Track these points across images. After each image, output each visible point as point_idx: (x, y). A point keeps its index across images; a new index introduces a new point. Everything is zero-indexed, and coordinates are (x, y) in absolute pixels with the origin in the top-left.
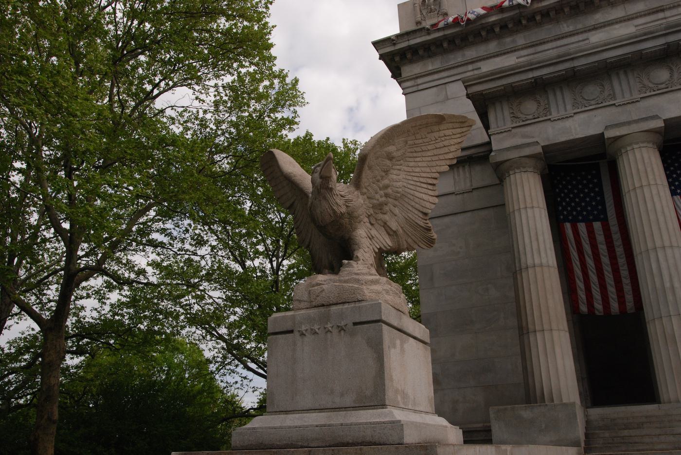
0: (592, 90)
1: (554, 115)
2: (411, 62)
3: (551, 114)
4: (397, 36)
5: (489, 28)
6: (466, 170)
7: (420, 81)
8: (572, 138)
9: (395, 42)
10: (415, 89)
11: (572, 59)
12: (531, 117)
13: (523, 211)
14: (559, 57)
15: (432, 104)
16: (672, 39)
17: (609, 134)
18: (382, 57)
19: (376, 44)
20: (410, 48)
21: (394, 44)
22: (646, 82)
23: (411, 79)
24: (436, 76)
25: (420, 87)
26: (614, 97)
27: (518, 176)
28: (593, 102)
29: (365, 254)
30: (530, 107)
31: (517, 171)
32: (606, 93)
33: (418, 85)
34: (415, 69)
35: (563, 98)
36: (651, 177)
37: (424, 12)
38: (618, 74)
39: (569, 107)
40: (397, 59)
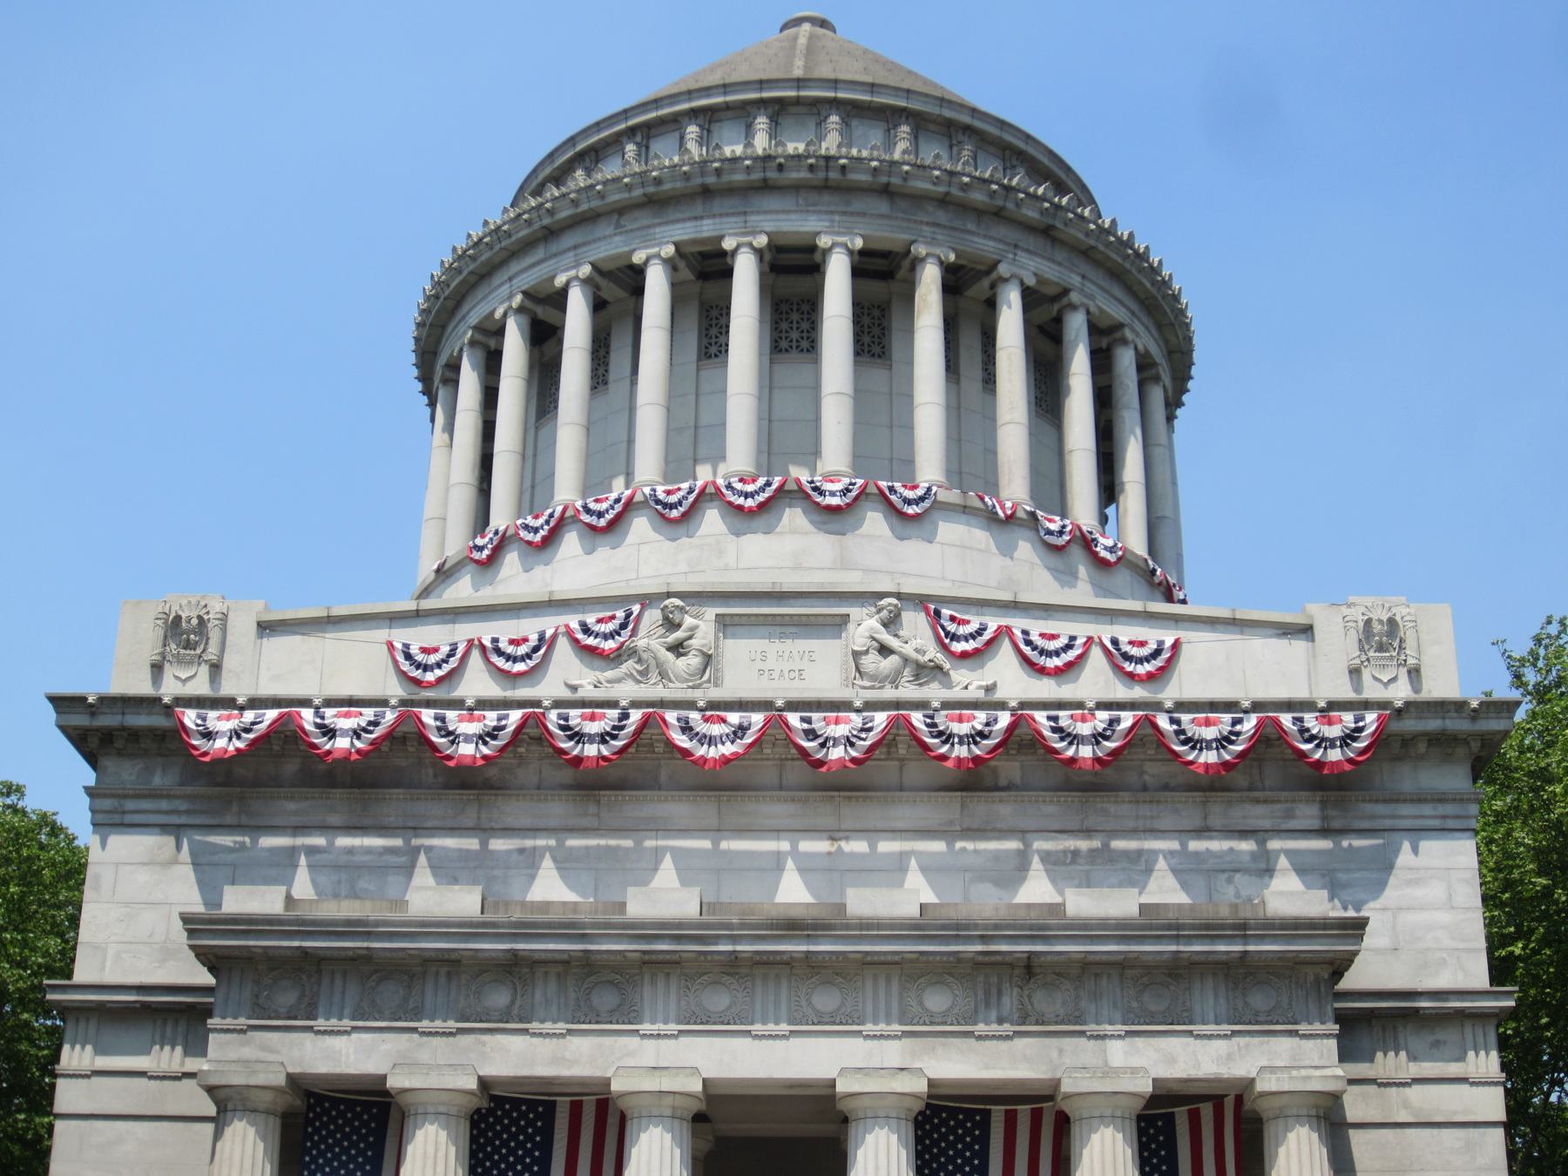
0: (391, 993)
2: (121, 754)
5: (288, 733)
6: (180, 1029)
7: (130, 805)
8: (338, 1070)
9: (94, 709)
10: (117, 818)
11: (369, 933)
14: (349, 922)
17: (393, 1083)
18: (63, 729)
19: (59, 702)
20: (123, 728)
21: (93, 714)
23: (113, 796)
24: (164, 805)
25: (128, 819)
33: (124, 812)
34: (126, 772)
35: (343, 993)
40: (94, 742)
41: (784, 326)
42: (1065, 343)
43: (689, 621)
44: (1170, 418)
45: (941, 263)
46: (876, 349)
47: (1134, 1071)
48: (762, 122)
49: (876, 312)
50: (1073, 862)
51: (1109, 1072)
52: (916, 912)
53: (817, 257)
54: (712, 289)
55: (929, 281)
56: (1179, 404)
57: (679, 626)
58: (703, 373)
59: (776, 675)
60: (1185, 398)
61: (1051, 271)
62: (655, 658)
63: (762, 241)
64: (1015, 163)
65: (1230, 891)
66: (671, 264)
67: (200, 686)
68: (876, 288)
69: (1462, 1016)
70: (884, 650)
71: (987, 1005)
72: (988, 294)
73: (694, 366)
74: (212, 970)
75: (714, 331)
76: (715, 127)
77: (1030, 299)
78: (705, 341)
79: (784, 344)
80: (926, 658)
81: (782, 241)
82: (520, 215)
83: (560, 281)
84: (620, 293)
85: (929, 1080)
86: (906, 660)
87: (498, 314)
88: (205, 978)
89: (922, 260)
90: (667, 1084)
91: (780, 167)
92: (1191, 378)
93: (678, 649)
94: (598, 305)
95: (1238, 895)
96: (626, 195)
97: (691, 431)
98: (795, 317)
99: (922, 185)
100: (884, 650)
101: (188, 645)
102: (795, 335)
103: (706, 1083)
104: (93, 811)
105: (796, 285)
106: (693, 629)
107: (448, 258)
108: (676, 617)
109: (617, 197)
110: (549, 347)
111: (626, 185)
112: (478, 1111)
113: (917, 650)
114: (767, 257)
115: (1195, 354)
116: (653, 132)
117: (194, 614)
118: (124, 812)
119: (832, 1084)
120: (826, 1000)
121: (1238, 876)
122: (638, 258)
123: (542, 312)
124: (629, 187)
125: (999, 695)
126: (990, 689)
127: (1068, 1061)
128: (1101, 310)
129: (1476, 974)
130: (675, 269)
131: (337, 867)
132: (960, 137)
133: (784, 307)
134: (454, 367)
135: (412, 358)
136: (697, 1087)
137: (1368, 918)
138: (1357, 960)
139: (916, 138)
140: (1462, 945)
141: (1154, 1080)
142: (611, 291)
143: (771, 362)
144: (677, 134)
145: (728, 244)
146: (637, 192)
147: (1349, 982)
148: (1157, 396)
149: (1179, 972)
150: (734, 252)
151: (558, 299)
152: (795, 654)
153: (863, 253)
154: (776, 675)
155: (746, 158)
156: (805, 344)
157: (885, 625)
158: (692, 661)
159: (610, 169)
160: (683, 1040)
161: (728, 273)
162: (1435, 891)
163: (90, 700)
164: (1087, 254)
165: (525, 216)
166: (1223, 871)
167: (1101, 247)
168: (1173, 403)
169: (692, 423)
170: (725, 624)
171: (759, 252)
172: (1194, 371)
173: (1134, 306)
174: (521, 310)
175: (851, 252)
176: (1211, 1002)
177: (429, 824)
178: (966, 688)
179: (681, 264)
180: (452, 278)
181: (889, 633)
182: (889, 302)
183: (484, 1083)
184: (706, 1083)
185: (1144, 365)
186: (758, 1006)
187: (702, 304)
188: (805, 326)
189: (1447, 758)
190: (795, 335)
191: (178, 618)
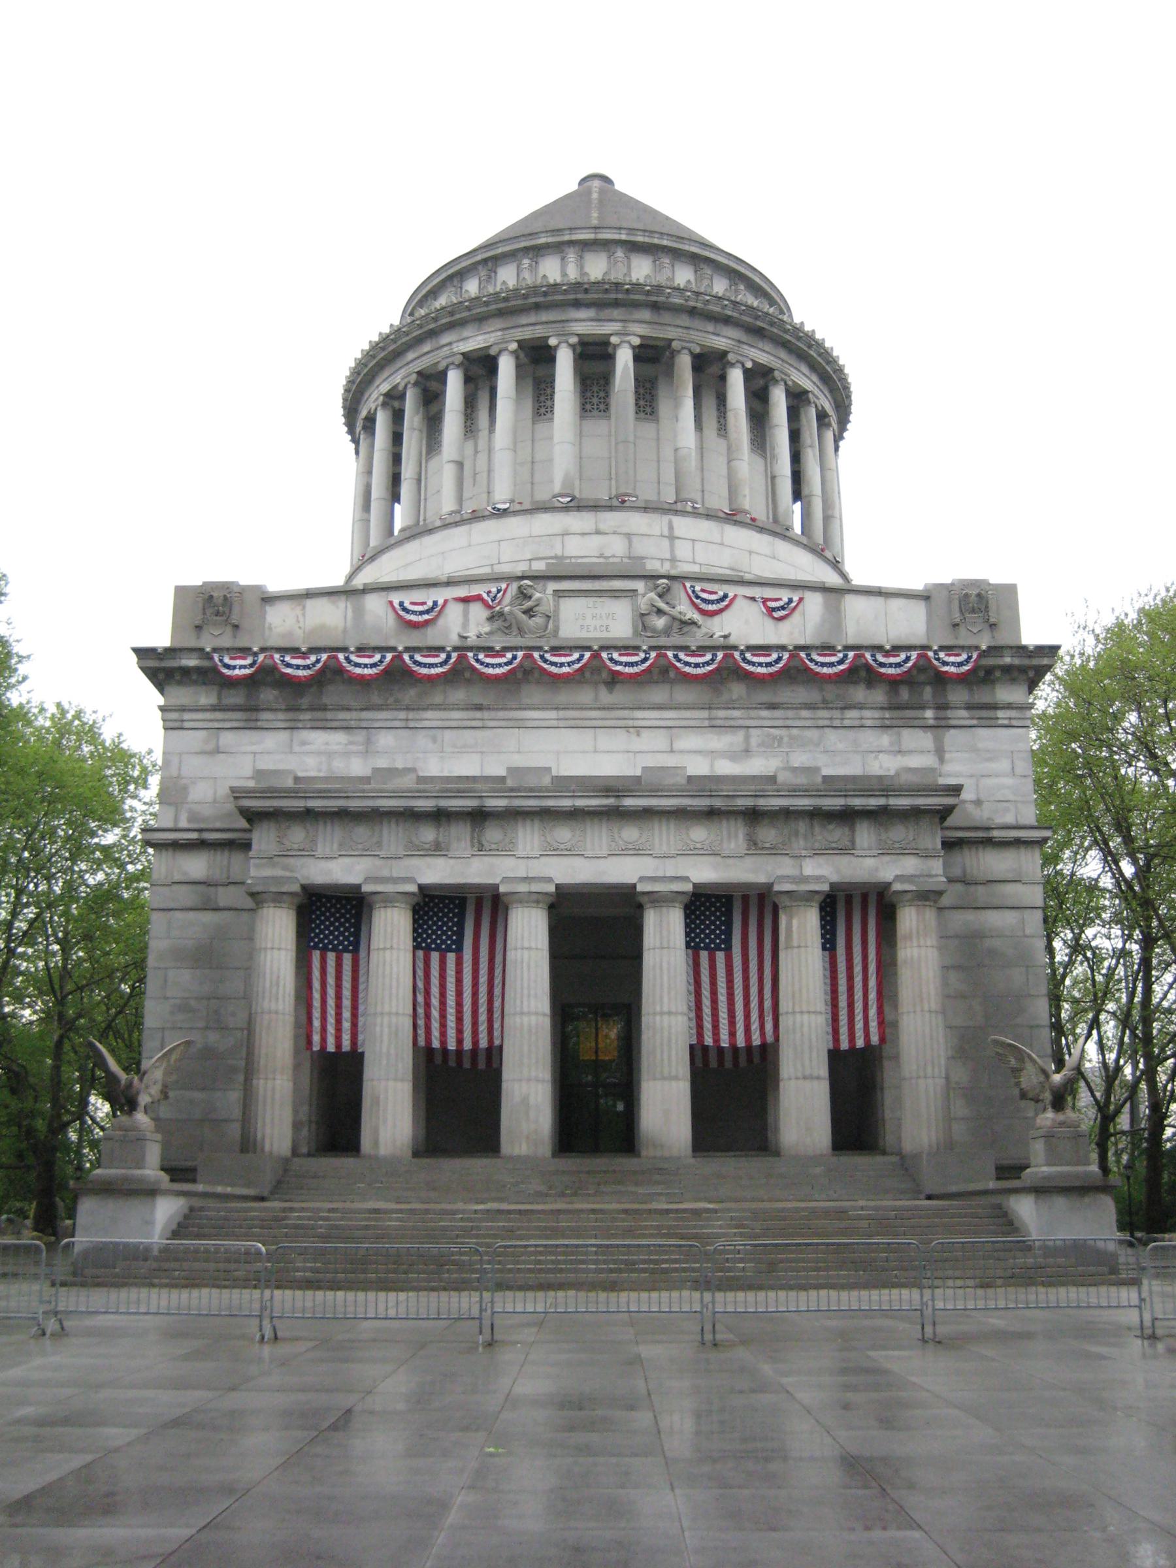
0: (361, 832)
1: (319, 852)
2: (180, 683)
3: (316, 851)
4: (167, 650)
7: (187, 716)
10: (177, 724)
12: (296, 846)
13: (269, 952)
15: (196, 753)
16: (443, 803)
17: (366, 888)
18: (142, 668)
19: (138, 651)
22: (414, 839)
23: (175, 710)
26: (379, 844)
27: (271, 910)
28: (360, 846)
29: (141, 1108)
30: (297, 835)
31: (272, 905)
32: (375, 840)
34: (183, 695)
36: (395, 941)
37: (209, 611)
38: (390, 822)
39: (335, 846)
40: (161, 676)
41: (589, 394)
42: (771, 402)
43: (537, 595)
44: (837, 449)
45: (691, 353)
46: (648, 410)
47: (818, 879)
48: (571, 256)
49: (648, 385)
50: (779, 746)
51: (805, 879)
52: (684, 781)
53: (610, 350)
54: (541, 371)
55: (685, 362)
56: (841, 438)
57: (530, 597)
58: (536, 426)
59: (592, 629)
60: (845, 434)
61: (763, 358)
62: (515, 618)
63: (574, 340)
64: (737, 281)
65: (876, 764)
66: (514, 353)
67: (226, 641)
68: (649, 369)
69: (1018, 843)
70: (660, 612)
71: (729, 837)
72: (720, 372)
73: (530, 422)
74: (249, 820)
75: (542, 398)
76: (540, 260)
77: (748, 375)
78: (537, 407)
79: (588, 407)
80: (687, 617)
81: (586, 339)
82: (414, 321)
83: (441, 367)
84: (481, 372)
85: (694, 884)
86: (674, 618)
87: (401, 388)
88: (243, 824)
89: (679, 352)
90: (535, 887)
91: (586, 291)
92: (849, 422)
93: (529, 612)
94: (468, 380)
95: (881, 767)
96: (485, 309)
97: (529, 465)
98: (595, 389)
99: (677, 301)
100: (660, 612)
101: (217, 614)
102: (595, 400)
103: (558, 886)
104: (164, 720)
105: (596, 367)
106: (539, 600)
107: (367, 347)
108: (529, 591)
109: (479, 310)
110: (434, 409)
111: (485, 302)
112: (418, 904)
113: (680, 613)
114: (579, 349)
115: (852, 407)
116: (498, 263)
117: (222, 594)
118: (183, 721)
119: (634, 886)
120: (630, 833)
121: (881, 755)
122: (493, 352)
123: (434, 385)
124: (486, 304)
125: (732, 640)
126: (725, 637)
127: (780, 872)
128: (794, 381)
129: (1029, 815)
130: (517, 358)
131: (319, 753)
132: (702, 266)
133: (588, 382)
134: (370, 420)
135: (341, 411)
136: (552, 889)
137: (962, 786)
138: (955, 810)
139: (673, 266)
140: (1019, 799)
141: (831, 884)
142: (478, 370)
143: (582, 418)
144: (515, 264)
145: (553, 342)
146: (493, 307)
147: (951, 821)
148: (829, 435)
149: (847, 817)
150: (556, 348)
151: (442, 377)
152: (604, 615)
153: (640, 346)
154: (592, 629)
155: (564, 285)
156: (602, 407)
157: (660, 596)
158: (539, 620)
159: (472, 287)
160: (543, 859)
161: (551, 360)
162: (1004, 765)
163: (159, 650)
164: (785, 345)
165: (418, 322)
166: (871, 752)
167: (793, 340)
168: (838, 438)
169: (530, 459)
170: (558, 594)
171: (573, 347)
172: (852, 418)
173: (815, 378)
174: (416, 384)
175: (633, 348)
176: (866, 836)
177: (377, 725)
178: (712, 636)
179: (522, 355)
180: (370, 361)
181: (663, 601)
182: (656, 378)
183: (421, 887)
184: (558, 886)
185: (822, 416)
186: (588, 840)
187: (535, 379)
188: (602, 394)
189: (1013, 680)
190: (595, 400)
191: (211, 597)
